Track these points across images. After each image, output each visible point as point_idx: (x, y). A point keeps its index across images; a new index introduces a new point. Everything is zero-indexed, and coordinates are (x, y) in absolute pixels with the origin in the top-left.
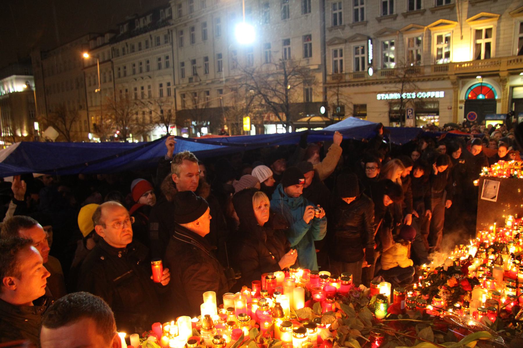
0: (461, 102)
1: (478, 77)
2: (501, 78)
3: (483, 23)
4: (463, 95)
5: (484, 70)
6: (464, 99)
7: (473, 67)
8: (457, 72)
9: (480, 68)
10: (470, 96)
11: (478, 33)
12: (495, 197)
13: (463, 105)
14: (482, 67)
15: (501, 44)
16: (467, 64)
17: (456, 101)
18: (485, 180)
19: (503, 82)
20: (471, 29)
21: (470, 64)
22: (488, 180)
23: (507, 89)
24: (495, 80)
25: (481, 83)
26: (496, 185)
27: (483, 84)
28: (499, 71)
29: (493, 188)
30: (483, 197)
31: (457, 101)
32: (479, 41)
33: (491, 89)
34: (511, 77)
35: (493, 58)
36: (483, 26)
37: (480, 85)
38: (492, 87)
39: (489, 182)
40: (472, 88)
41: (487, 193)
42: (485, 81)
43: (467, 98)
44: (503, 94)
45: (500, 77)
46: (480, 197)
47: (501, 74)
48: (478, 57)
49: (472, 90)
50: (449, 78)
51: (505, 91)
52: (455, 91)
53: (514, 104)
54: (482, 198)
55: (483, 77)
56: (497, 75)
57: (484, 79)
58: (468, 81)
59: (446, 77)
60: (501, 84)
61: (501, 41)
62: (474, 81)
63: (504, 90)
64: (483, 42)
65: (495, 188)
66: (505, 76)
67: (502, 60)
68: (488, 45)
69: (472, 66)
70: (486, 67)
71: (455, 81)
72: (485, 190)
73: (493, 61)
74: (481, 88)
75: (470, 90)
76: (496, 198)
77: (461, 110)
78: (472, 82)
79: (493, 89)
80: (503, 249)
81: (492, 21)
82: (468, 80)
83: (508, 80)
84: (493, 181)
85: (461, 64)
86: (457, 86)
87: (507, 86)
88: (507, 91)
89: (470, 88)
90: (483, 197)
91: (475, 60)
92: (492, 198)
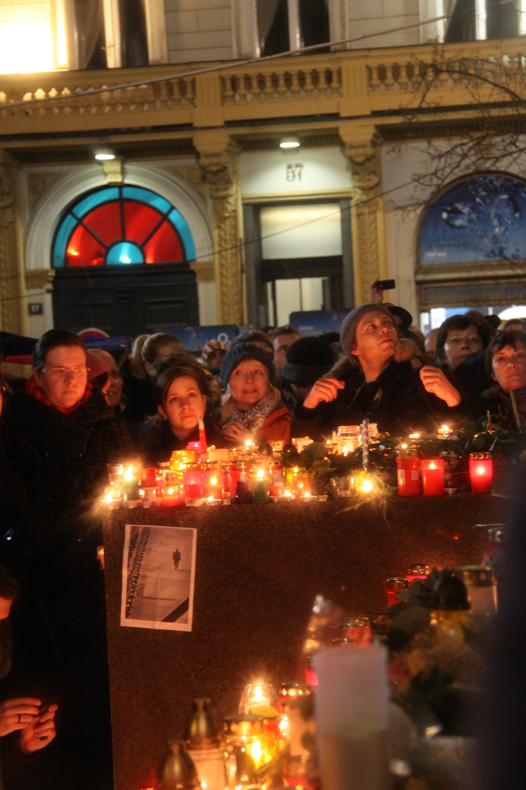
1: (102, 156)
2: (204, 161)
5: (123, 124)
6: (47, 265)
9: (107, 109)
10: (73, 252)
12: (184, 607)
14: (113, 104)
16: (47, 90)
18: (128, 528)
22: (141, 527)
23: (235, 211)
24: (176, 172)
25: (121, 186)
26: (181, 550)
27: (127, 193)
28: (189, 126)
29: (172, 561)
30: (127, 616)
31: (16, 277)
33: (164, 217)
35: (158, 65)
37: (113, 194)
38: (172, 208)
39: (146, 532)
40: (82, 210)
41: (146, 592)
43: (59, 263)
45: (198, 155)
46: (119, 619)
49: (80, 221)
54: (126, 622)
58: (58, 177)
60: (206, 188)
62: (87, 177)
63: (222, 219)
65: (180, 563)
66: (217, 155)
69: (66, 97)
70: (133, 108)
72: (133, 579)
75: (70, 222)
76: (190, 613)
77: (36, 319)
78: (73, 184)
79: (174, 217)
80: (194, 728)
82: (57, 168)
83: (235, 172)
84: (168, 529)
86: (8, 201)
87: (231, 200)
88: (235, 227)
89: (69, 210)
90: (127, 616)
91: (80, 70)
92: (171, 618)
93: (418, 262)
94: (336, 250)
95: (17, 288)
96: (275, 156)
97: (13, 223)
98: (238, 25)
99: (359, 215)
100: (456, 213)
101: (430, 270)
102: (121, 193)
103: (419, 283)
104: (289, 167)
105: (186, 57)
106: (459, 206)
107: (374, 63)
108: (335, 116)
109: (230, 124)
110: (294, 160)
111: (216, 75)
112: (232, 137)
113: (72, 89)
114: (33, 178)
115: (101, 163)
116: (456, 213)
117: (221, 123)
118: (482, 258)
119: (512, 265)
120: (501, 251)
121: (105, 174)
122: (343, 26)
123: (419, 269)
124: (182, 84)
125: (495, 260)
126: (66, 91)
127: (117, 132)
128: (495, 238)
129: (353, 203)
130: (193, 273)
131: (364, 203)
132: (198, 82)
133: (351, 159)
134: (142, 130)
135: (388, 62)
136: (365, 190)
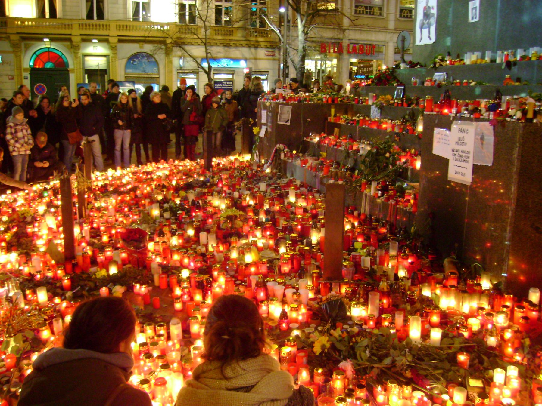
0: (26, 70)
1: (45, 40)
4: (29, 62)
7: (36, 27)
8: (19, 31)
13: (27, 74)
17: (20, 68)
19: (74, 48)
21: (32, 22)
24: (64, 45)
25: (49, 48)
27: (51, 50)
28: (70, 35)
31: (21, 69)
34: (83, 44)
37: (47, 50)
40: (38, 53)
42: (54, 46)
44: (76, 63)
47: (74, 39)
50: (8, 38)
51: (78, 60)
52: (16, 56)
53: (86, 76)
55: (52, 40)
56: (70, 40)
57: (53, 43)
58: (33, 44)
59: (3, 36)
60: (72, 50)
62: (40, 45)
67: (74, 22)
71: (17, 42)
73: (60, 21)
74: (50, 55)
75: (35, 56)
77: (26, 80)
82: (32, 42)
85: (23, 20)
88: (80, 60)
89: (35, 53)
93: (125, 72)
95: (21, 72)
96: (91, 44)
97: (20, 56)
98: (81, 11)
100: (134, 61)
101: (128, 74)
103: (125, 77)
105: (68, 17)
106: (135, 59)
107: (118, 23)
108: (108, 35)
109: (81, 35)
110: (95, 45)
113: (35, 22)
114: (25, 44)
115: (45, 42)
116: (134, 61)
117: (79, 34)
118: (141, 73)
119: (148, 74)
120: (145, 71)
121: (46, 45)
122: (108, 14)
123: (125, 74)
125: (143, 73)
126: (34, 23)
127: (52, 34)
128: (143, 68)
129: (110, 57)
130: (68, 71)
131: (114, 57)
133: (111, 46)
134: (55, 34)
135: (122, 24)
136: (114, 54)
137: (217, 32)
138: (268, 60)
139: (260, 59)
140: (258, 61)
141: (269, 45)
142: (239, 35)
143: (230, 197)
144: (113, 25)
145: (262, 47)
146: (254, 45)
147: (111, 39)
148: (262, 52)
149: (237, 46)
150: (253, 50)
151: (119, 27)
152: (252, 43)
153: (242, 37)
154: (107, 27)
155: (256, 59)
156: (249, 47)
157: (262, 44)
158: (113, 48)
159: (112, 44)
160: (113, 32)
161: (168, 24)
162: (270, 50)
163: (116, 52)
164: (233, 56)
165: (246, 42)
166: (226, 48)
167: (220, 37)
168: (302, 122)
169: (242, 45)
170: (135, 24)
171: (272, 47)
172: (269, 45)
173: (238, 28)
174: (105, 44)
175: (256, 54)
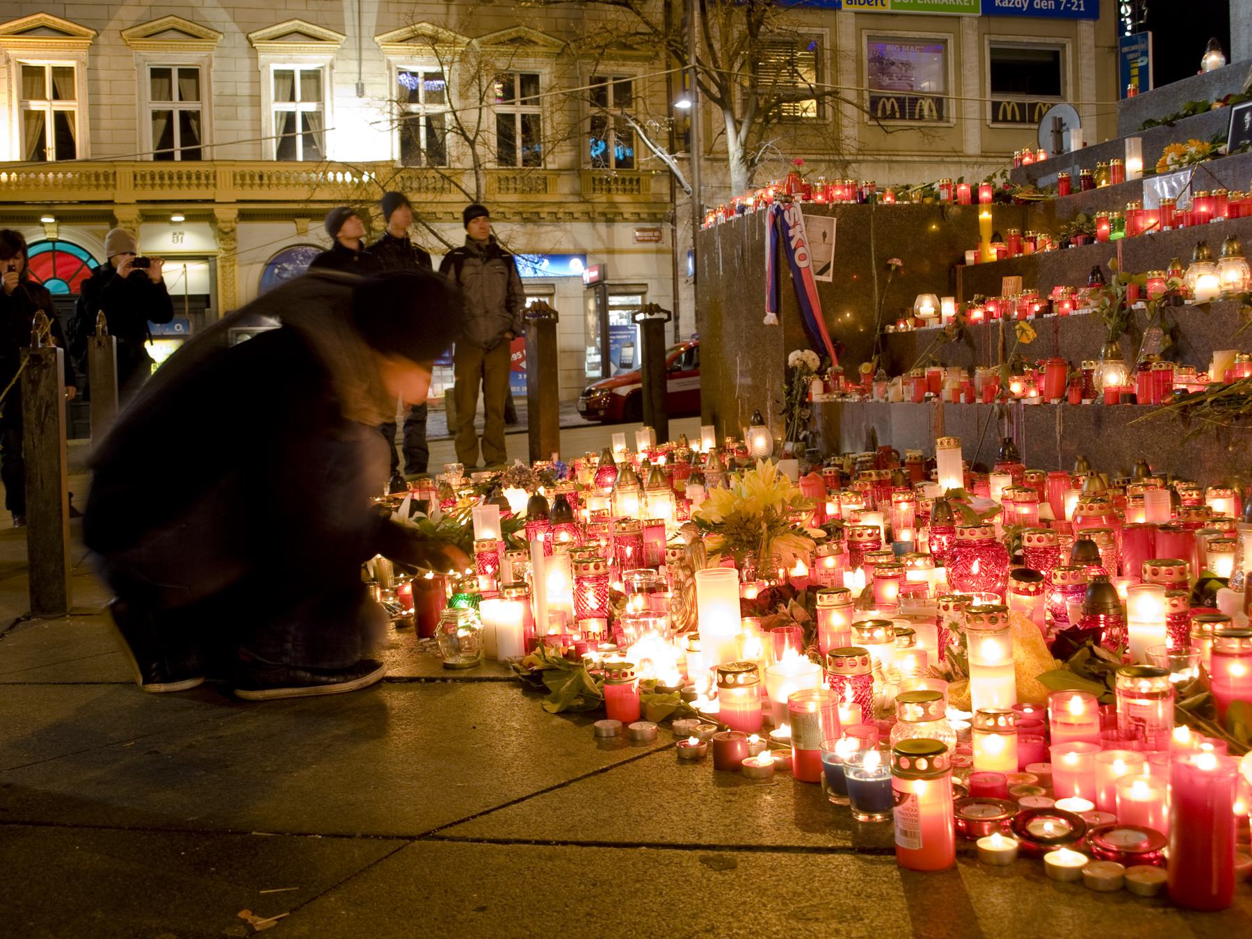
3: (47, 47)
11: (31, 75)
15: (105, 124)
20: (8, 61)
25: (54, 241)
27: (59, 246)
28: (111, 202)
32: (35, 105)
34: (145, 228)
36: (47, 57)
37: (49, 246)
42: (68, 234)
47: (119, 212)
48: (36, 152)
55: (61, 219)
56: (110, 218)
57: (64, 228)
61: (104, 113)
64: (47, 107)
68: (62, 120)
73: (84, 169)
81: (74, 47)
94: (204, 291)
96: (166, 225)
98: (140, 141)
99: (223, 267)
102: (54, 246)
104: (175, 234)
107: (238, 170)
108: (212, 201)
109: (139, 202)
110: (177, 229)
111: (131, 169)
112: (140, 210)
115: (42, 224)
124: (106, 176)
132: (118, 175)
134: (70, 203)
135: (247, 170)
137: (503, 184)
138: (645, 252)
139: (622, 252)
140: (617, 257)
141: (644, 212)
142: (563, 188)
143: (956, 203)
144: (225, 175)
145: (626, 220)
146: (604, 214)
147: (219, 211)
148: (626, 234)
149: (558, 219)
150: (602, 227)
151: (241, 179)
152: (600, 209)
153: (572, 194)
154: (210, 179)
155: (610, 252)
156: (590, 218)
157: (628, 210)
158: (225, 235)
159: (221, 225)
160: (226, 191)
161: (373, 166)
162: (648, 226)
163: (235, 244)
164: (547, 246)
165: (583, 207)
166: (530, 226)
167: (514, 197)
168: (875, 272)
169: (572, 217)
170: (284, 167)
171: (654, 218)
172: (644, 212)
173: (559, 172)
174: (205, 226)
175: (611, 236)
